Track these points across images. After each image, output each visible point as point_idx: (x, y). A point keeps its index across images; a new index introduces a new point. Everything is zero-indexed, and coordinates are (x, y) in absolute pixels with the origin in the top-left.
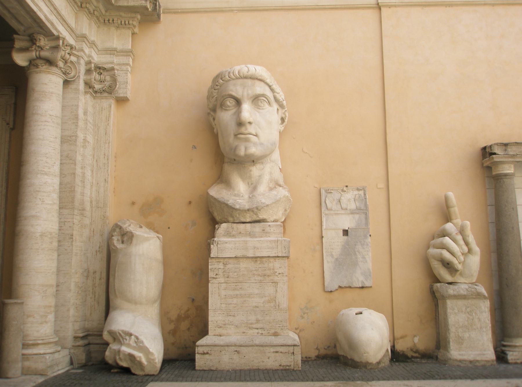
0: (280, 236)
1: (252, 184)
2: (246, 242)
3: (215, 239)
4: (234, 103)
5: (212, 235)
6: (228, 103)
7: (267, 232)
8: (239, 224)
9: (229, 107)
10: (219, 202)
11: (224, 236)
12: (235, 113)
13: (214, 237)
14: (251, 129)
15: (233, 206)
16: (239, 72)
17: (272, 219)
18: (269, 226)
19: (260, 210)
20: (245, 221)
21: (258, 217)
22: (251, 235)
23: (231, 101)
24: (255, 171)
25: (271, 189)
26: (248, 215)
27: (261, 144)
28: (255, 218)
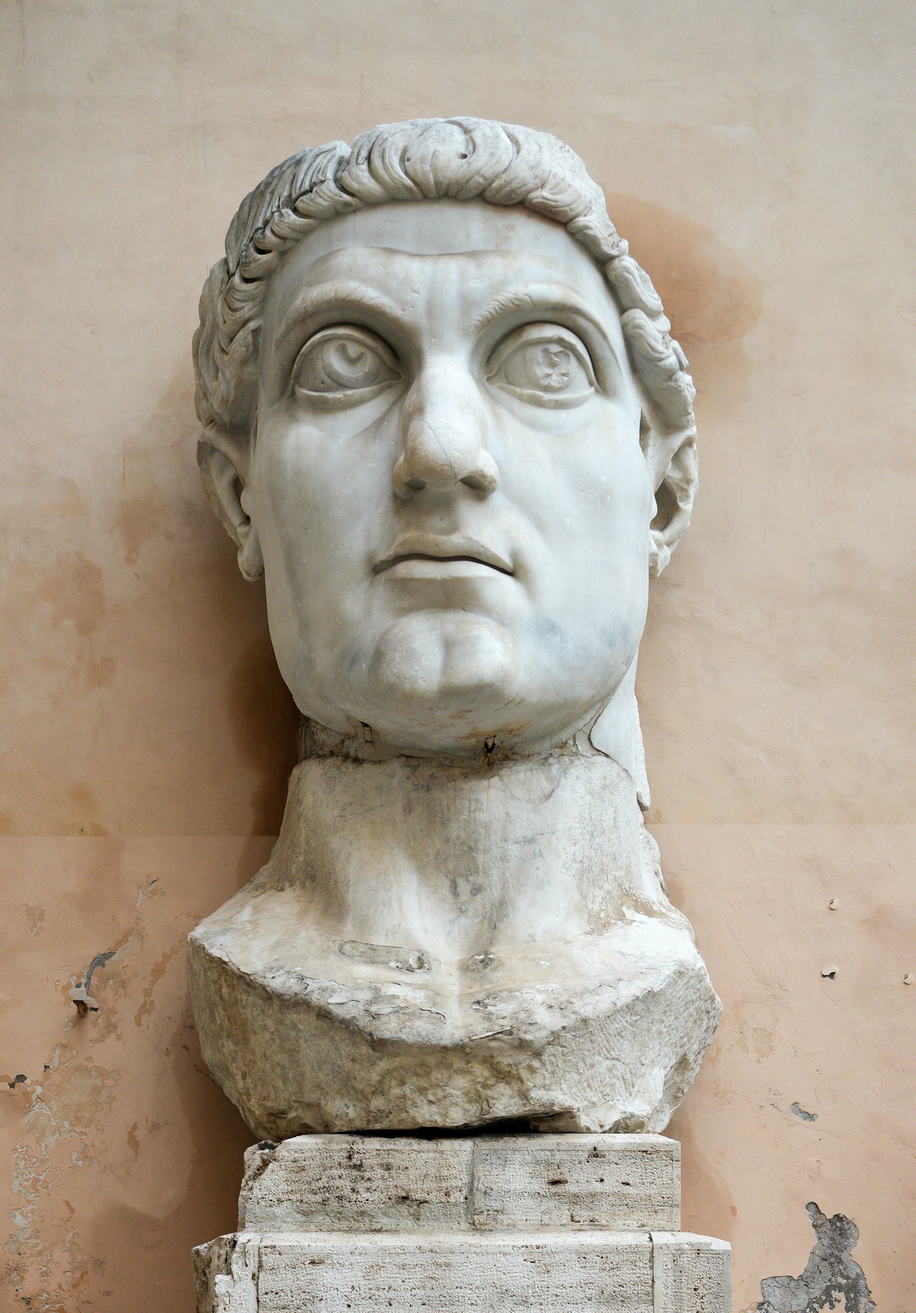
0: (660, 1220)
1: (477, 890)
2: (441, 1262)
3: (242, 1237)
4: (369, 363)
5: (219, 1206)
6: (335, 362)
7: (575, 1199)
8: (401, 1143)
9: (341, 385)
10: (269, 996)
11: (307, 1215)
12: (379, 424)
13: (233, 1223)
14: (487, 527)
15: (364, 1022)
16: (403, 159)
17: (614, 1117)
18: (595, 1153)
19: (538, 1054)
20: (440, 1122)
21: (524, 1095)
22: (476, 1212)
23: (353, 350)
24: (498, 802)
25: (599, 926)
26: (461, 1082)
27: (547, 628)
28: (505, 1104)
